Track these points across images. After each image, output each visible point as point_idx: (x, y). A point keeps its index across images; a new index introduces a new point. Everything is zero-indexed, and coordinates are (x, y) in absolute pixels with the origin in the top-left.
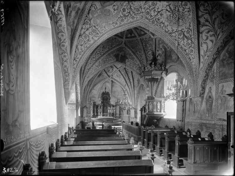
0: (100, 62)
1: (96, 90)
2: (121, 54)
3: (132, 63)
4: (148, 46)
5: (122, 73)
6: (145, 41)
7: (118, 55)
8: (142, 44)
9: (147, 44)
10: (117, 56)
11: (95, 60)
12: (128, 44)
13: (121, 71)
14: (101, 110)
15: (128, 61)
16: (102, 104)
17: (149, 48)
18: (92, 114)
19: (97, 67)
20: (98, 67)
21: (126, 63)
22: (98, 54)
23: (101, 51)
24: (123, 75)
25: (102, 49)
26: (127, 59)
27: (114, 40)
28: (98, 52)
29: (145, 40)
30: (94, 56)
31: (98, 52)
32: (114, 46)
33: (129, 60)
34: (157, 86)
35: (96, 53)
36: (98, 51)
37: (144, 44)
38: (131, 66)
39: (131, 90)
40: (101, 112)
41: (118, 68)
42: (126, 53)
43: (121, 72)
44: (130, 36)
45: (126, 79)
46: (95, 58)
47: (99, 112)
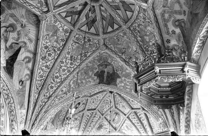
0: (70, 85)
2: (106, 70)
3: (128, 84)
4: (147, 38)
5: (133, 122)
6: (139, 32)
7: (103, 72)
8: (135, 37)
9: (145, 37)
10: (100, 75)
11: (59, 82)
12: (112, 45)
13: (130, 118)
15: (122, 82)
17: (151, 44)
19: (64, 93)
21: (116, 85)
22: (64, 70)
23: (69, 66)
24: (135, 124)
25: (70, 61)
26: (119, 77)
27: (88, 43)
28: (63, 68)
29: (139, 29)
30: (58, 74)
31: (63, 68)
32: (89, 53)
33: (123, 78)
34: (187, 118)
35: (61, 70)
36: (62, 65)
37: (140, 39)
38: (127, 88)
41: (126, 114)
42: (115, 67)
43: (132, 120)
44: (112, 30)
46: (60, 78)
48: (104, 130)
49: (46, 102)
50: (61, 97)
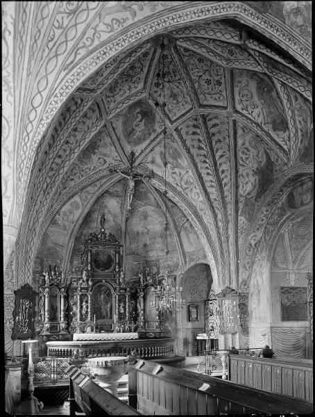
1: (65, 229)
5: (188, 143)
13: (183, 132)
14: (88, 307)
16: (90, 283)
18: (47, 325)
20: (135, 14)
24: (192, 151)
39: (220, 216)
40: (84, 312)
45: (203, 172)
48: (99, 158)
49: (64, 26)
50: (118, 20)
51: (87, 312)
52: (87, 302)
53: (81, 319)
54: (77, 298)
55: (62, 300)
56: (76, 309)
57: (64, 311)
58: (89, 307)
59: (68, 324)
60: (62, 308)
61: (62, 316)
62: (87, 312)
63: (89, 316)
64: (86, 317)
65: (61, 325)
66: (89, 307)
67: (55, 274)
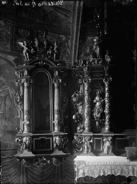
40: (96, 115)
47: (86, 121)
51: (103, 115)
52: (102, 96)
53: (93, 128)
54: (85, 89)
55: (56, 91)
56: (84, 110)
57: (59, 112)
58: (107, 106)
59: (70, 136)
60: (56, 108)
61: (56, 121)
62: (103, 115)
63: (107, 123)
64: (102, 125)
65: (54, 138)
66: (107, 106)
67: (41, 44)
